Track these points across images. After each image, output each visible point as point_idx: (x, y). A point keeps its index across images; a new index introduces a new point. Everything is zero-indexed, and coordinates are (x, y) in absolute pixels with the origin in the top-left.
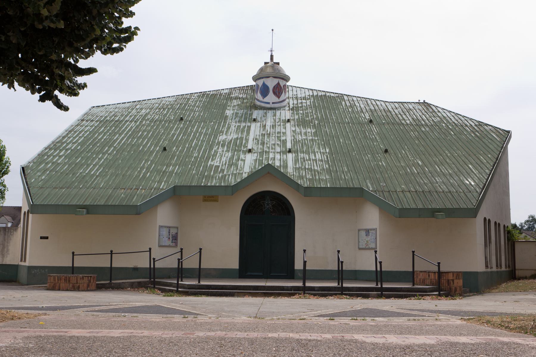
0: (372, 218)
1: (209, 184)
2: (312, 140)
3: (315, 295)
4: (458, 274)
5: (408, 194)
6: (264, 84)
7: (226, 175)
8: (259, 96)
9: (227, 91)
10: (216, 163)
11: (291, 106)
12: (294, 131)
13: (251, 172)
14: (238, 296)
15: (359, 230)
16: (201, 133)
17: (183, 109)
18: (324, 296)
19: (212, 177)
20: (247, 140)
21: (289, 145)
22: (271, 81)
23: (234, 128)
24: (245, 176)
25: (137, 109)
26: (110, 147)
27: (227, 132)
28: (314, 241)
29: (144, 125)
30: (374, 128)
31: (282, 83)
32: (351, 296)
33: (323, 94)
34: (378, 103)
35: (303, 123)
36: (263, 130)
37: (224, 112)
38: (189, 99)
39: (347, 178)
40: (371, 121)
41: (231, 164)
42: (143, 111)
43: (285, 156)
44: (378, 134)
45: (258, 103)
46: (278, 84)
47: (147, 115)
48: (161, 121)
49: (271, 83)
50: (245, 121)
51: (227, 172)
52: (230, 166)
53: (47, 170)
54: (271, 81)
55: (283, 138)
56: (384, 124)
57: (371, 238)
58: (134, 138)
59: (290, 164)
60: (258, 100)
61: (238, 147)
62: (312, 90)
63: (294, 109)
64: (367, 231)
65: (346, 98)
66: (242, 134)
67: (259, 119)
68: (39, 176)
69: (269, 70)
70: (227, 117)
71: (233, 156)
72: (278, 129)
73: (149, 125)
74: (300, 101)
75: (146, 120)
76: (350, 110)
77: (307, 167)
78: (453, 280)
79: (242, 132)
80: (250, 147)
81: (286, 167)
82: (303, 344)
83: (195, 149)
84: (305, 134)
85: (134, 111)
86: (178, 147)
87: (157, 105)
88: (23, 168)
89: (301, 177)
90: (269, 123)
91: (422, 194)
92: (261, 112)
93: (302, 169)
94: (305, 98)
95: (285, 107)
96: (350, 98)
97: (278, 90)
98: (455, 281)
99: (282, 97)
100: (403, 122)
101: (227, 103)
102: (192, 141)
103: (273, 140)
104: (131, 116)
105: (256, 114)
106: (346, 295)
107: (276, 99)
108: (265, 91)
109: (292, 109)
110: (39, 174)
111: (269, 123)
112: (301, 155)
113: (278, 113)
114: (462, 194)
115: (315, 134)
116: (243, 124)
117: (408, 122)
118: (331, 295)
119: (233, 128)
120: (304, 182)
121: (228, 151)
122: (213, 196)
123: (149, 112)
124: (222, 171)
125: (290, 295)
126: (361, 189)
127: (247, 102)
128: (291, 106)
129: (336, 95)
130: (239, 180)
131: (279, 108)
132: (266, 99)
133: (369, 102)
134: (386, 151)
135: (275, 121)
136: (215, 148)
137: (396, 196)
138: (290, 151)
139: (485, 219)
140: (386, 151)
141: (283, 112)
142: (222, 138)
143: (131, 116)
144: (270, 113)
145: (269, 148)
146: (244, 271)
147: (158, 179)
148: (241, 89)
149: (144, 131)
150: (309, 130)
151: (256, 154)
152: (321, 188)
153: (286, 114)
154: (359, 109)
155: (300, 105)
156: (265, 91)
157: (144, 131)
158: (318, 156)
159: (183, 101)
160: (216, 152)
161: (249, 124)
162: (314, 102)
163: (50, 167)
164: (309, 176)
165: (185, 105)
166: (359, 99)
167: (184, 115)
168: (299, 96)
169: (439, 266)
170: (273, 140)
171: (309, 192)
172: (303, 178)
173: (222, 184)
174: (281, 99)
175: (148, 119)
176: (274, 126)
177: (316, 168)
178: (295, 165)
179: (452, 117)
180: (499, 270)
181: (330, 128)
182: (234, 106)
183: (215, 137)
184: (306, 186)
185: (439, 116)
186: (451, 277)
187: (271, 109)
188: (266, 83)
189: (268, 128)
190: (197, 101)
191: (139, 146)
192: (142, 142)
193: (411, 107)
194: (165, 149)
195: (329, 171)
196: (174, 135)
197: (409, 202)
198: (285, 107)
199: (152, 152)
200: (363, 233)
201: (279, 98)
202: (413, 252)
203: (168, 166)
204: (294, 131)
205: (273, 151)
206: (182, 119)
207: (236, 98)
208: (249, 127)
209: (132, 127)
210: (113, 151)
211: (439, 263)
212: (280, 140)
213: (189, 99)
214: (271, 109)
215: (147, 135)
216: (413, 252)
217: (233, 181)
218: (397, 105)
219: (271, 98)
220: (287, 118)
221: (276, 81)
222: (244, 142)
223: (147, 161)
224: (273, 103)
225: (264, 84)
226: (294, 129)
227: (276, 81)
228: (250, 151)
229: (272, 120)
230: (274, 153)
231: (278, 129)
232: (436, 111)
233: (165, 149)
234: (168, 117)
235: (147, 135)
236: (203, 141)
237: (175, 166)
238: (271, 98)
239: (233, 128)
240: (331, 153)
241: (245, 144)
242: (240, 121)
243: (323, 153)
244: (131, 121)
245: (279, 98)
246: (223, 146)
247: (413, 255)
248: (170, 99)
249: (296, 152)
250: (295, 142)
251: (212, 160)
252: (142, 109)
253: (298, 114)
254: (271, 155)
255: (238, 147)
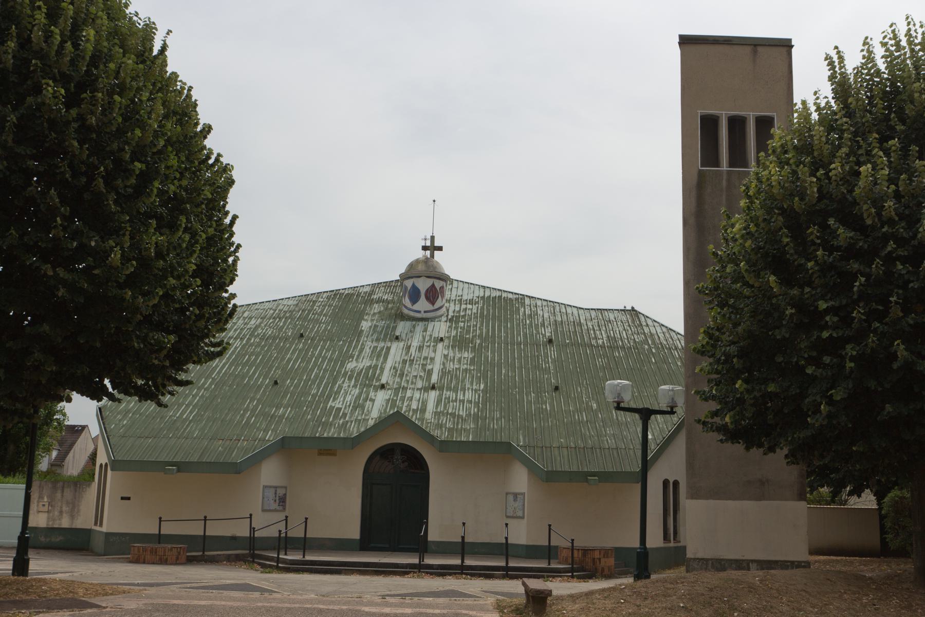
0: (520, 479)
1: (325, 435)
2: (466, 369)
3: (431, 574)
4: (606, 552)
5: (565, 450)
6: (414, 286)
7: (347, 422)
8: (407, 301)
9: (367, 289)
10: (338, 404)
11: (451, 314)
12: (446, 356)
13: (380, 417)
14: (346, 574)
15: (507, 494)
16: (324, 358)
17: (305, 319)
18: (442, 575)
19: (331, 425)
20: (382, 370)
21: (434, 378)
22: (425, 282)
23: (368, 350)
24: (371, 423)
25: (245, 318)
26: (207, 379)
27: (358, 356)
28: (453, 506)
29: (252, 345)
30: (552, 352)
31: (438, 284)
32: (472, 575)
33: (498, 294)
34: (569, 310)
35: (460, 343)
36: (406, 354)
37: (359, 324)
38: (315, 302)
39: (498, 427)
40: (550, 341)
41: (358, 405)
42: (253, 322)
43: (426, 394)
44: (554, 361)
45: (405, 311)
46: (433, 285)
47: (257, 327)
48: (274, 338)
49: (423, 285)
50: (384, 340)
51: (350, 417)
52: (355, 408)
53: (128, 411)
54: (425, 282)
55: (429, 367)
56: (566, 345)
57: (518, 504)
58: (238, 365)
59: (431, 406)
60: (406, 307)
61: (369, 380)
62: (484, 287)
63: (453, 320)
64: (516, 495)
65: (527, 301)
66: (377, 360)
67: (404, 336)
68: (120, 420)
69: (421, 267)
70: (362, 331)
71: (360, 394)
72: (424, 354)
73: (259, 344)
74: (463, 306)
75: (256, 337)
76: (528, 322)
77: (450, 411)
78: (600, 559)
79: (379, 356)
80: (384, 381)
81: (423, 410)
82: (320, 611)
83: (314, 382)
84: (460, 360)
85: (241, 321)
86: (293, 379)
87: (272, 312)
88: (100, 409)
89: (440, 426)
90: (415, 344)
91: (582, 450)
92: (408, 324)
93: (443, 415)
94: (471, 302)
95: (441, 316)
96: (533, 302)
97: (433, 295)
98: (603, 560)
99: (438, 303)
100: (594, 342)
101: (365, 308)
102: (312, 370)
103: (416, 370)
104: (236, 330)
105: (402, 328)
106: (467, 574)
107: (429, 307)
108: (415, 295)
109: (451, 320)
110: (119, 417)
111: (415, 344)
112: (447, 393)
113: (430, 325)
114: (631, 452)
115: (472, 362)
116: (381, 344)
117: (600, 342)
118: (450, 574)
119: (367, 350)
120: (442, 433)
121: (355, 386)
122: (328, 449)
123: (260, 323)
124: (345, 415)
125: (403, 574)
126: (509, 444)
127: (392, 308)
128: (451, 314)
129: (515, 296)
130: (362, 429)
131: (432, 319)
132: (416, 307)
133: (557, 309)
134: (557, 388)
135: (424, 338)
136: (339, 382)
137: (549, 454)
138: (433, 388)
139: (666, 483)
140: (557, 388)
141: (437, 324)
142: (351, 365)
143: (236, 330)
144: (420, 326)
145: (408, 381)
146: (366, 543)
147: (263, 426)
148: (388, 284)
149: (252, 354)
150: (466, 355)
151: (390, 392)
152: (461, 442)
153: (440, 328)
154: (540, 320)
155: (462, 314)
156: (415, 295)
157: (252, 354)
158: (469, 395)
159: (308, 301)
160: (340, 387)
161: (389, 344)
162: (482, 308)
163: (133, 407)
164: (449, 425)
165: (309, 311)
166: (545, 303)
167: (306, 328)
168: (465, 298)
169: (572, 543)
170: (416, 370)
171: (445, 447)
172: (441, 427)
173: (342, 435)
174: (437, 305)
175: (258, 335)
176: (420, 348)
177: (461, 413)
178: (437, 408)
179: (661, 335)
180: (672, 544)
181: (493, 352)
182: (374, 314)
183: (342, 365)
184: (443, 438)
185: (644, 333)
186: (597, 555)
187: (422, 319)
188: (417, 285)
189: (413, 350)
190: (324, 306)
191: (243, 378)
192: (248, 371)
193: (612, 318)
194: (276, 383)
195: (476, 417)
196: (290, 360)
197: (564, 464)
198: (441, 316)
199: (260, 387)
200: (511, 498)
201: (433, 304)
202: (550, 526)
203: (278, 408)
204: (446, 356)
205: (413, 386)
206: (302, 335)
207: (379, 301)
208: (389, 349)
209: (236, 348)
210: (211, 384)
211: (573, 540)
212: (425, 370)
213: (315, 302)
214: (422, 319)
215: (256, 360)
216: (550, 526)
217: (355, 429)
218: (593, 314)
219: (423, 304)
220: (441, 335)
221: (429, 282)
222: (378, 372)
223: (252, 400)
224: (425, 312)
225: (414, 286)
226: (446, 352)
227: (429, 282)
228: (383, 387)
229: (421, 338)
230: (413, 389)
231: (424, 354)
232: (644, 324)
233: (276, 383)
234: (285, 332)
235: (256, 360)
236: (326, 370)
237: (286, 407)
238: (423, 304)
239: (367, 350)
240: (485, 391)
241: (379, 375)
242: (378, 340)
243: (476, 390)
244: (236, 339)
245: (433, 304)
246: (350, 379)
247: (550, 529)
248: (290, 302)
249: (441, 389)
250: (444, 373)
251: (334, 401)
252: (251, 318)
253: (456, 328)
254: (409, 393)
255: (369, 380)
